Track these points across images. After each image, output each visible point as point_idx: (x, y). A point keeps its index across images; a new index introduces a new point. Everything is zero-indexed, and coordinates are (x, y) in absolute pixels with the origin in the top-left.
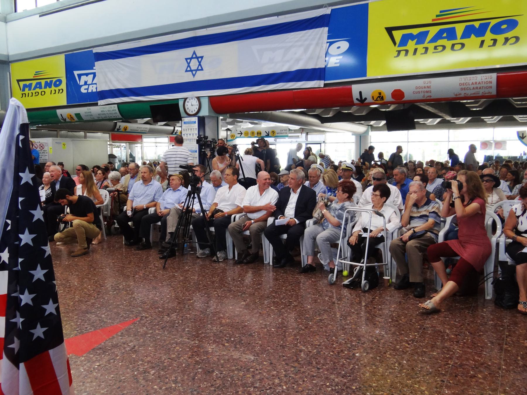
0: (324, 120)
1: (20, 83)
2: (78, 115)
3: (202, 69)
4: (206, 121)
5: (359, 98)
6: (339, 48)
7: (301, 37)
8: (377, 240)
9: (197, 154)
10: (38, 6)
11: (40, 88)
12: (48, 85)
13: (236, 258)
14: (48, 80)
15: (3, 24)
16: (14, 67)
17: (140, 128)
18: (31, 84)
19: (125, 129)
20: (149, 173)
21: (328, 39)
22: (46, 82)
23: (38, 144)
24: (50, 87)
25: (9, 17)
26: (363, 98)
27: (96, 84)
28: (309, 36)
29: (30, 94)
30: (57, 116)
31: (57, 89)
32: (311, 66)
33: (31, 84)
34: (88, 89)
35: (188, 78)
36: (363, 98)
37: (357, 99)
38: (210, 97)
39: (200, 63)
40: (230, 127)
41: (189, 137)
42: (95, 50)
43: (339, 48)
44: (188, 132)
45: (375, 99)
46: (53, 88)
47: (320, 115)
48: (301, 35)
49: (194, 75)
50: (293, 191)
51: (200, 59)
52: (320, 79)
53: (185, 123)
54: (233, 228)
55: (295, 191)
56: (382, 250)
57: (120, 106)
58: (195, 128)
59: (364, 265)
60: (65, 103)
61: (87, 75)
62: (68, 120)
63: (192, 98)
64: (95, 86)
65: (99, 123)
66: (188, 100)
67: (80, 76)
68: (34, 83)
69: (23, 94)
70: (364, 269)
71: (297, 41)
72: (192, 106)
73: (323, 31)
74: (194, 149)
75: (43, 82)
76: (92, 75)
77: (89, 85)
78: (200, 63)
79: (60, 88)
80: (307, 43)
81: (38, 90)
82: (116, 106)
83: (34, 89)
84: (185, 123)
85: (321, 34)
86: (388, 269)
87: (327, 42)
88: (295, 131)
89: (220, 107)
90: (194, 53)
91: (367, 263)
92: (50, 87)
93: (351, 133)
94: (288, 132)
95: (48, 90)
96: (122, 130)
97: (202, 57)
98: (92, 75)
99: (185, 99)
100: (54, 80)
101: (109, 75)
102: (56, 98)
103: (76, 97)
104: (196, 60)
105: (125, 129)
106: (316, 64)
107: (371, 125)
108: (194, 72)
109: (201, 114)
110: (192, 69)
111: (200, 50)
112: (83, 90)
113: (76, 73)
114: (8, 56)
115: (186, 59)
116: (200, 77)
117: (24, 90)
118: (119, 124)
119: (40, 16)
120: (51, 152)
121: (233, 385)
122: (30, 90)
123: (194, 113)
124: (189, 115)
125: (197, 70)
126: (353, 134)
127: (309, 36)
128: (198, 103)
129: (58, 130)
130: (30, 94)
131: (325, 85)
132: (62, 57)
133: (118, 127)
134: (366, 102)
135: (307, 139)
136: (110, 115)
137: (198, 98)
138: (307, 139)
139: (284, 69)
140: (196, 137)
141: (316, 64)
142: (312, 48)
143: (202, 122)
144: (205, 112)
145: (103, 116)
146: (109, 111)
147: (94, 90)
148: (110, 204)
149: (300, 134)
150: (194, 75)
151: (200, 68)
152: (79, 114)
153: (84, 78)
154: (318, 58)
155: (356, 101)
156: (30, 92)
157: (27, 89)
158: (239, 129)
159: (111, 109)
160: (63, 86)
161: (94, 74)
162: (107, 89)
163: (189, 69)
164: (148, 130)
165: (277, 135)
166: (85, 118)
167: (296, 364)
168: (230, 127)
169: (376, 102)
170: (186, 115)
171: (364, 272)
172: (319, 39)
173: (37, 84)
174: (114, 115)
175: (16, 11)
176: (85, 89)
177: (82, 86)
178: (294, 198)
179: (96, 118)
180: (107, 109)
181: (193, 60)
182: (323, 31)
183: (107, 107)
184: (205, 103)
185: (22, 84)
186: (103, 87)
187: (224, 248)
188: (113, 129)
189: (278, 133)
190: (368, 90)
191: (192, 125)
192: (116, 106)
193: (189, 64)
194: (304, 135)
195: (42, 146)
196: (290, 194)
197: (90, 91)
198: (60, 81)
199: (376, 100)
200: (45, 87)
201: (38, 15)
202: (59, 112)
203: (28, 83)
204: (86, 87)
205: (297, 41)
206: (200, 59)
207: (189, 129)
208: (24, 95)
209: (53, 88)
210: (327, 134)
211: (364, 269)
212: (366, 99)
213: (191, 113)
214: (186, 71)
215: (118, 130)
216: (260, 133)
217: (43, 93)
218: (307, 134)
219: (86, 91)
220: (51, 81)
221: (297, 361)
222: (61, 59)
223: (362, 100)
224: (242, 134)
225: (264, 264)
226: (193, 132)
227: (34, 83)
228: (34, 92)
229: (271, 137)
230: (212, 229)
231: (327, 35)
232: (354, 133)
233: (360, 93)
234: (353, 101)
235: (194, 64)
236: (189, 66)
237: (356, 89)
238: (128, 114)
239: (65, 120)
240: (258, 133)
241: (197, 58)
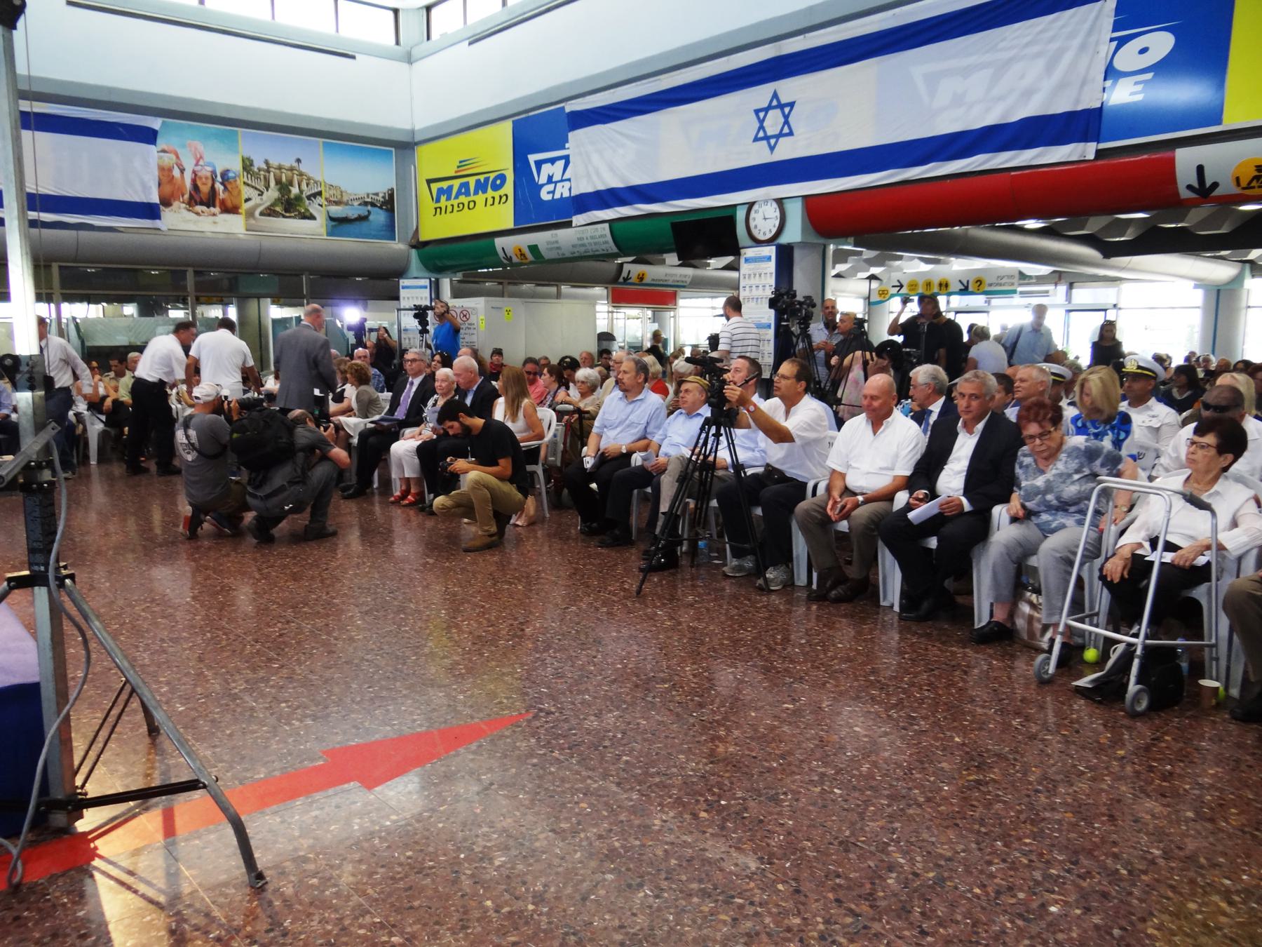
0: (1110, 251)
2: (534, 249)
3: (791, 133)
4: (797, 254)
5: (1196, 185)
6: (1143, 51)
7: (1041, 32)
8: (1185, 578)
9: (770, 333)
10: (469, 22)
11: (467, 194)
12: (481, 187)
13: (814, 586)
14: (482, 178)
15: (405, 66)
16: (422, 152)
17: (672, 275)
18: (451, 188)
19: (641, 278)
20: (633, 373)
21: (1114, 31)
22: (478, 181)
23: (458, 311)
24: (485, 191)
25: (416, 53)
26: (1208, 183)
27: (569, 180)
28: (1063, 26)
29: (449, 209)
30: (496, 253)
31: (496, 194)
32: (1061, 106)
33: (451, 188)
34: (553, 192)
35: (759, 155)
36: (1208, 183)
37: (1189, 187)
38: (808, 200)
39: (786, 117)
40: (875, 270)
41: (755, 293)
42: (570, 107)
43: (1143, 51)
44: (753, 282)
45: (1244, 184)
46: (490, 193)
47: (1099, 236)
48: (1040, 28)
49: (772, 148)
50: (965, 425)
51: (787, 110)
52: (1085, 139)
53: (747, 260)
54: (807, 512)
55: (969, 429)
56: (1204, 603)
57: (616, 225)
58: (768, 271)
59: (1138, 641)
60: (509, 224)
61: (552, 161)
62: (515, 260)
63: (766, 202)
64: (567, 184)
65: (581, 263)
66: (756, 207)
67: (539, 164)
68: (456, 184)
70: (1139, 652)
71: (1027, 45)
72: (764, 221)
73: (1100, 10)
74: (765, 321)
75: (472, 181)
76: (563, 162)
77: (556, 183)
78: (786, 117)
79: (502, 192)
80: (1054, 46)
81: (463, 199)
82: (607, 225)
83: (457, 197)
84: (747, 260)
85: (1097, 18)
86: (1217, 659)
87: (1112, 40)
88: (1041, 280)
89: (828, 220)
90: (775, 96)
91: (1147, 637)
92: (485, 191)
93: (1192, 283)
94: (1016, 280)
95: (480, 198)
96: (634, 279)
97: (792, 105)
98: (563, 162)
99: (751, 205)
100: (492, 176)
101: (598, 160)
102: (493, 215)
103: (534, 211)
104: (778, 111)
105: (641, 278)
106: (1077, 101)
107: (1251, 262)
108: (773, 141)
109: (784, 240)
110: (769, 133)
111: (789, 88)
112: (545, 195)
113: (532, 158)
114: (413, 132)
115: (757, 112)
116: (787, 151)
117: (438, 201)
118: (626, 268)
119: (470, 44)
120: (482, 326)
121: (674, 937)
122: (448, 199)
123: (769, 236)
124: (759, 243)
125: (781, 135)
126: (1196, 287)
127: (1063, 26)
128: (778, 213)
129: (506, 281)
130: (449, 209)
131: (1100, 154)
132: (508, 126)
133: (624, 274)
134: (1217, 192)
135: (1069, 297)
136: (594, 248)
137: (780, 202)
138: (1069, 297)
139: (991, 119)
140: (769, 293)
141: (1077, 101)
142: (1067, 58)
143: (785, 257)
144: (793, 234)
145: (582, 249)
146: (592, 237)
147: (566, 194)
148: (560, 439)
149: (1050, 288)
150: (772, 148)
151: (786, 130)
152: (536, 246)
153: (547, 169)
154: (1084, 83)
155: (1185, 194)
156: (449, 203)
157: (443, 198)
158: (896, 276)
159: (597, 234)
160: (509, 188)
161: (567, 159)
162: (590, 190)
163: (761, 134)
164: (689, 280)
165: (987, 289)
166: (547, 255)
167: (864, 908)
168: (875, 270)
169: (1248, 192)
170: (750, 242)
171: (1136, 662)
172: (1090, 32)
173: (462, 185)
174: (604, 247)
177: (543, 185)
178: (965, 446)
179: (568, 255)
180: (589, 235)
181: (771, 113)
182: (1100, 10)
183: (589, 229)
184: (796, 213)
185: (435, 187)
186: (584, 186)
187: (785, 557)
188: (615, 280)
189: (990, 285)
190: (1224, 162)
191: (763, 265)
192: (607, 225)
193: (761, 122)
194: (1062, 289)
195: (465, 314)
196: (957, 434)
197: (557, 196)
198: (502, 178)
199: (1249, 187)
200: (476, 193)
202: (499, 242)
203: (445, 185)
204: (551, 187)
205: (1027, 45)
206: (786, 108)
207: (757, 275)
209: (490, 193)
210: (1125, 286)
211: (1139, 652)
212: (1215, 185)
213: (761, 237)
214: (756, 139)
215: (626, 279)
216: (947, 285)
217: (472, 205)
218: (1071, 286)
219: (549, 197)
220: (487, 179)
221: (870, 897)
222: (505, 131)
223: (1204, 190)
224: (901, 286)
225: (878, 606)
226: (763, 281)
227: (456, 184)
228: (455, 202)
229: (972, 293)
230: (759, 511)
231: (1112, 20)
232: (1200, 283)
233: (1200, 169)
234: (1177, 194)
235: (774, 122)
236: (761, 127)
237: (1186, 160)
238: (636, 242)
239: (510, 259)
240: (940, 285)
241: (781, 106)
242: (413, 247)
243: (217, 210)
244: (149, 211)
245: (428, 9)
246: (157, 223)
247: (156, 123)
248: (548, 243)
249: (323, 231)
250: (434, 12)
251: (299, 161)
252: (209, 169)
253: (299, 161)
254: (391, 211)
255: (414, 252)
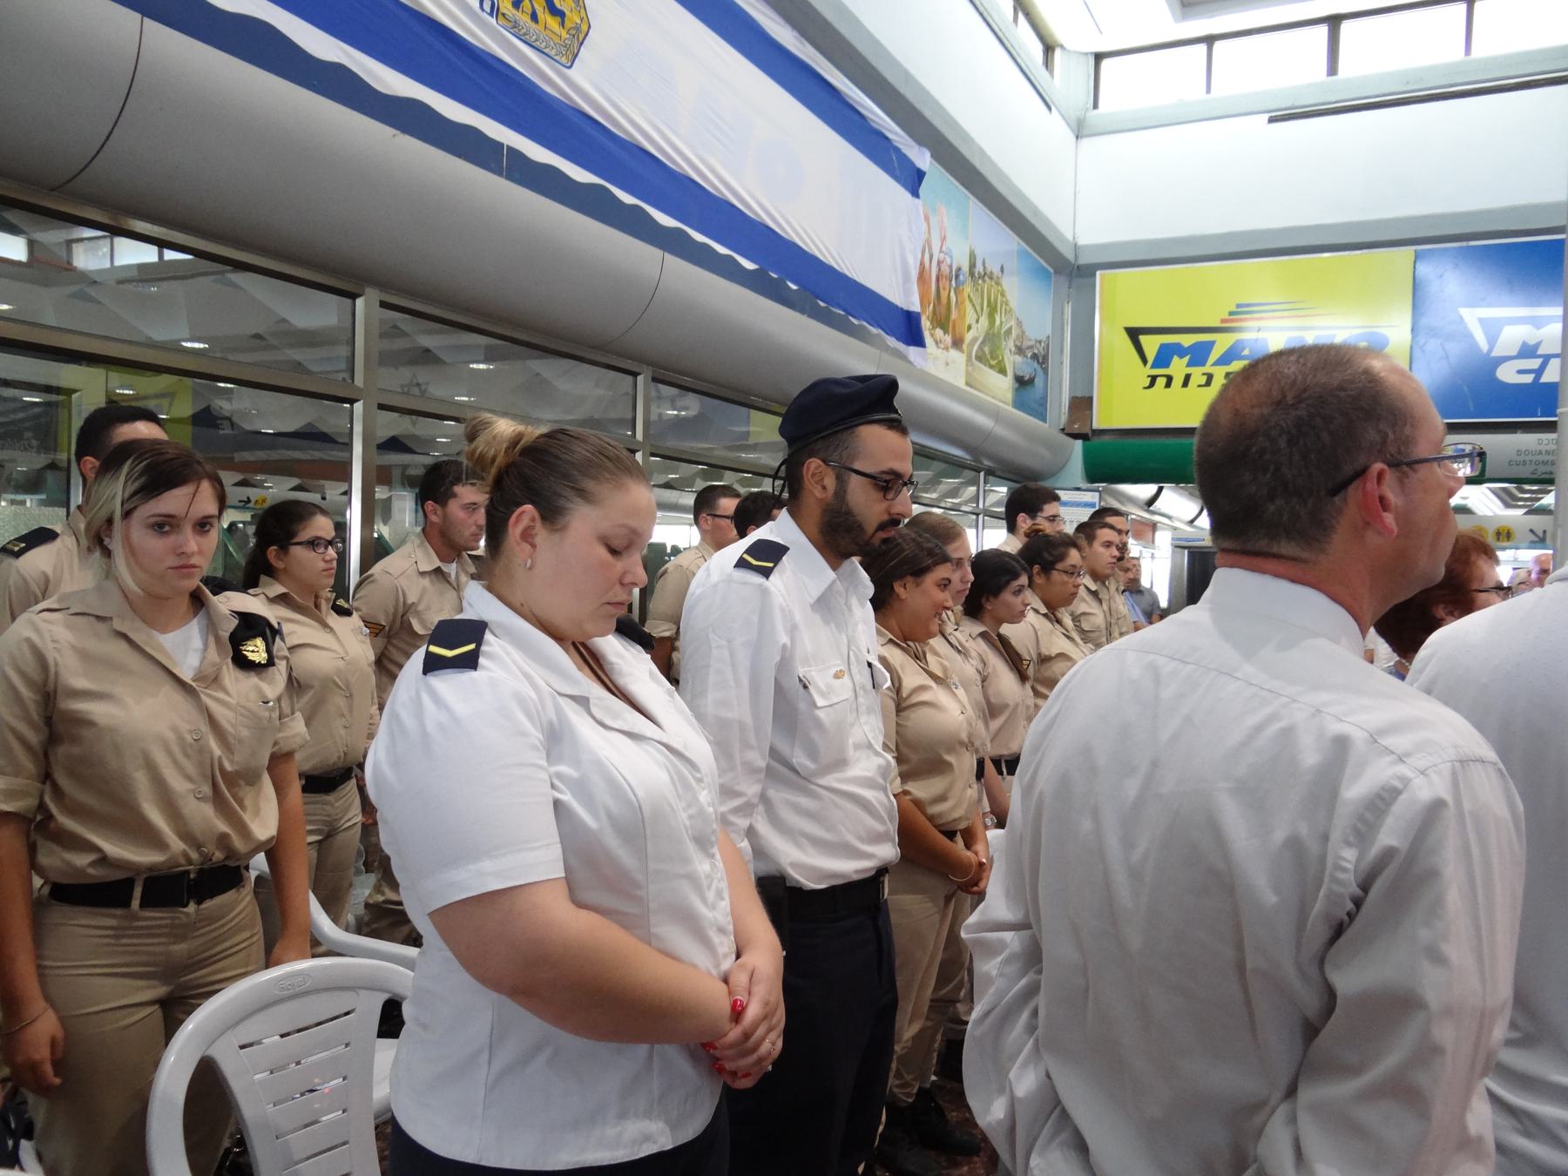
1: (1143, 339)
34: (1539, 372)
69: (1154, 379)
77: (1547, 358)
119: (1272, 120)
156: (1198, 375)
175: (1096, 106)
176: (1520, 372)
201: (1266, 117)
203: (1187, 340)
208: (1161, 382)
219: (1529, 379)
242: (1075, 436)
243: (948, 339)
244: (909, 329)
245: (1099, 57)
246: (912, 352)
247: (922, 158)
248: (1519, 453)
249: (1009, 396)
250: (1105, 63)
251: (1002, 270)
252: (948, 261)
253: (1002, 270)
254: (1046, 371)
255: (1079, 443)
